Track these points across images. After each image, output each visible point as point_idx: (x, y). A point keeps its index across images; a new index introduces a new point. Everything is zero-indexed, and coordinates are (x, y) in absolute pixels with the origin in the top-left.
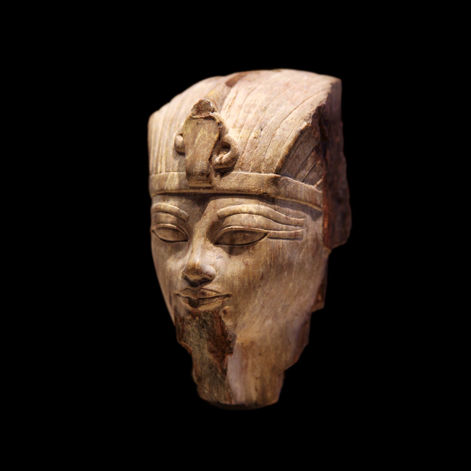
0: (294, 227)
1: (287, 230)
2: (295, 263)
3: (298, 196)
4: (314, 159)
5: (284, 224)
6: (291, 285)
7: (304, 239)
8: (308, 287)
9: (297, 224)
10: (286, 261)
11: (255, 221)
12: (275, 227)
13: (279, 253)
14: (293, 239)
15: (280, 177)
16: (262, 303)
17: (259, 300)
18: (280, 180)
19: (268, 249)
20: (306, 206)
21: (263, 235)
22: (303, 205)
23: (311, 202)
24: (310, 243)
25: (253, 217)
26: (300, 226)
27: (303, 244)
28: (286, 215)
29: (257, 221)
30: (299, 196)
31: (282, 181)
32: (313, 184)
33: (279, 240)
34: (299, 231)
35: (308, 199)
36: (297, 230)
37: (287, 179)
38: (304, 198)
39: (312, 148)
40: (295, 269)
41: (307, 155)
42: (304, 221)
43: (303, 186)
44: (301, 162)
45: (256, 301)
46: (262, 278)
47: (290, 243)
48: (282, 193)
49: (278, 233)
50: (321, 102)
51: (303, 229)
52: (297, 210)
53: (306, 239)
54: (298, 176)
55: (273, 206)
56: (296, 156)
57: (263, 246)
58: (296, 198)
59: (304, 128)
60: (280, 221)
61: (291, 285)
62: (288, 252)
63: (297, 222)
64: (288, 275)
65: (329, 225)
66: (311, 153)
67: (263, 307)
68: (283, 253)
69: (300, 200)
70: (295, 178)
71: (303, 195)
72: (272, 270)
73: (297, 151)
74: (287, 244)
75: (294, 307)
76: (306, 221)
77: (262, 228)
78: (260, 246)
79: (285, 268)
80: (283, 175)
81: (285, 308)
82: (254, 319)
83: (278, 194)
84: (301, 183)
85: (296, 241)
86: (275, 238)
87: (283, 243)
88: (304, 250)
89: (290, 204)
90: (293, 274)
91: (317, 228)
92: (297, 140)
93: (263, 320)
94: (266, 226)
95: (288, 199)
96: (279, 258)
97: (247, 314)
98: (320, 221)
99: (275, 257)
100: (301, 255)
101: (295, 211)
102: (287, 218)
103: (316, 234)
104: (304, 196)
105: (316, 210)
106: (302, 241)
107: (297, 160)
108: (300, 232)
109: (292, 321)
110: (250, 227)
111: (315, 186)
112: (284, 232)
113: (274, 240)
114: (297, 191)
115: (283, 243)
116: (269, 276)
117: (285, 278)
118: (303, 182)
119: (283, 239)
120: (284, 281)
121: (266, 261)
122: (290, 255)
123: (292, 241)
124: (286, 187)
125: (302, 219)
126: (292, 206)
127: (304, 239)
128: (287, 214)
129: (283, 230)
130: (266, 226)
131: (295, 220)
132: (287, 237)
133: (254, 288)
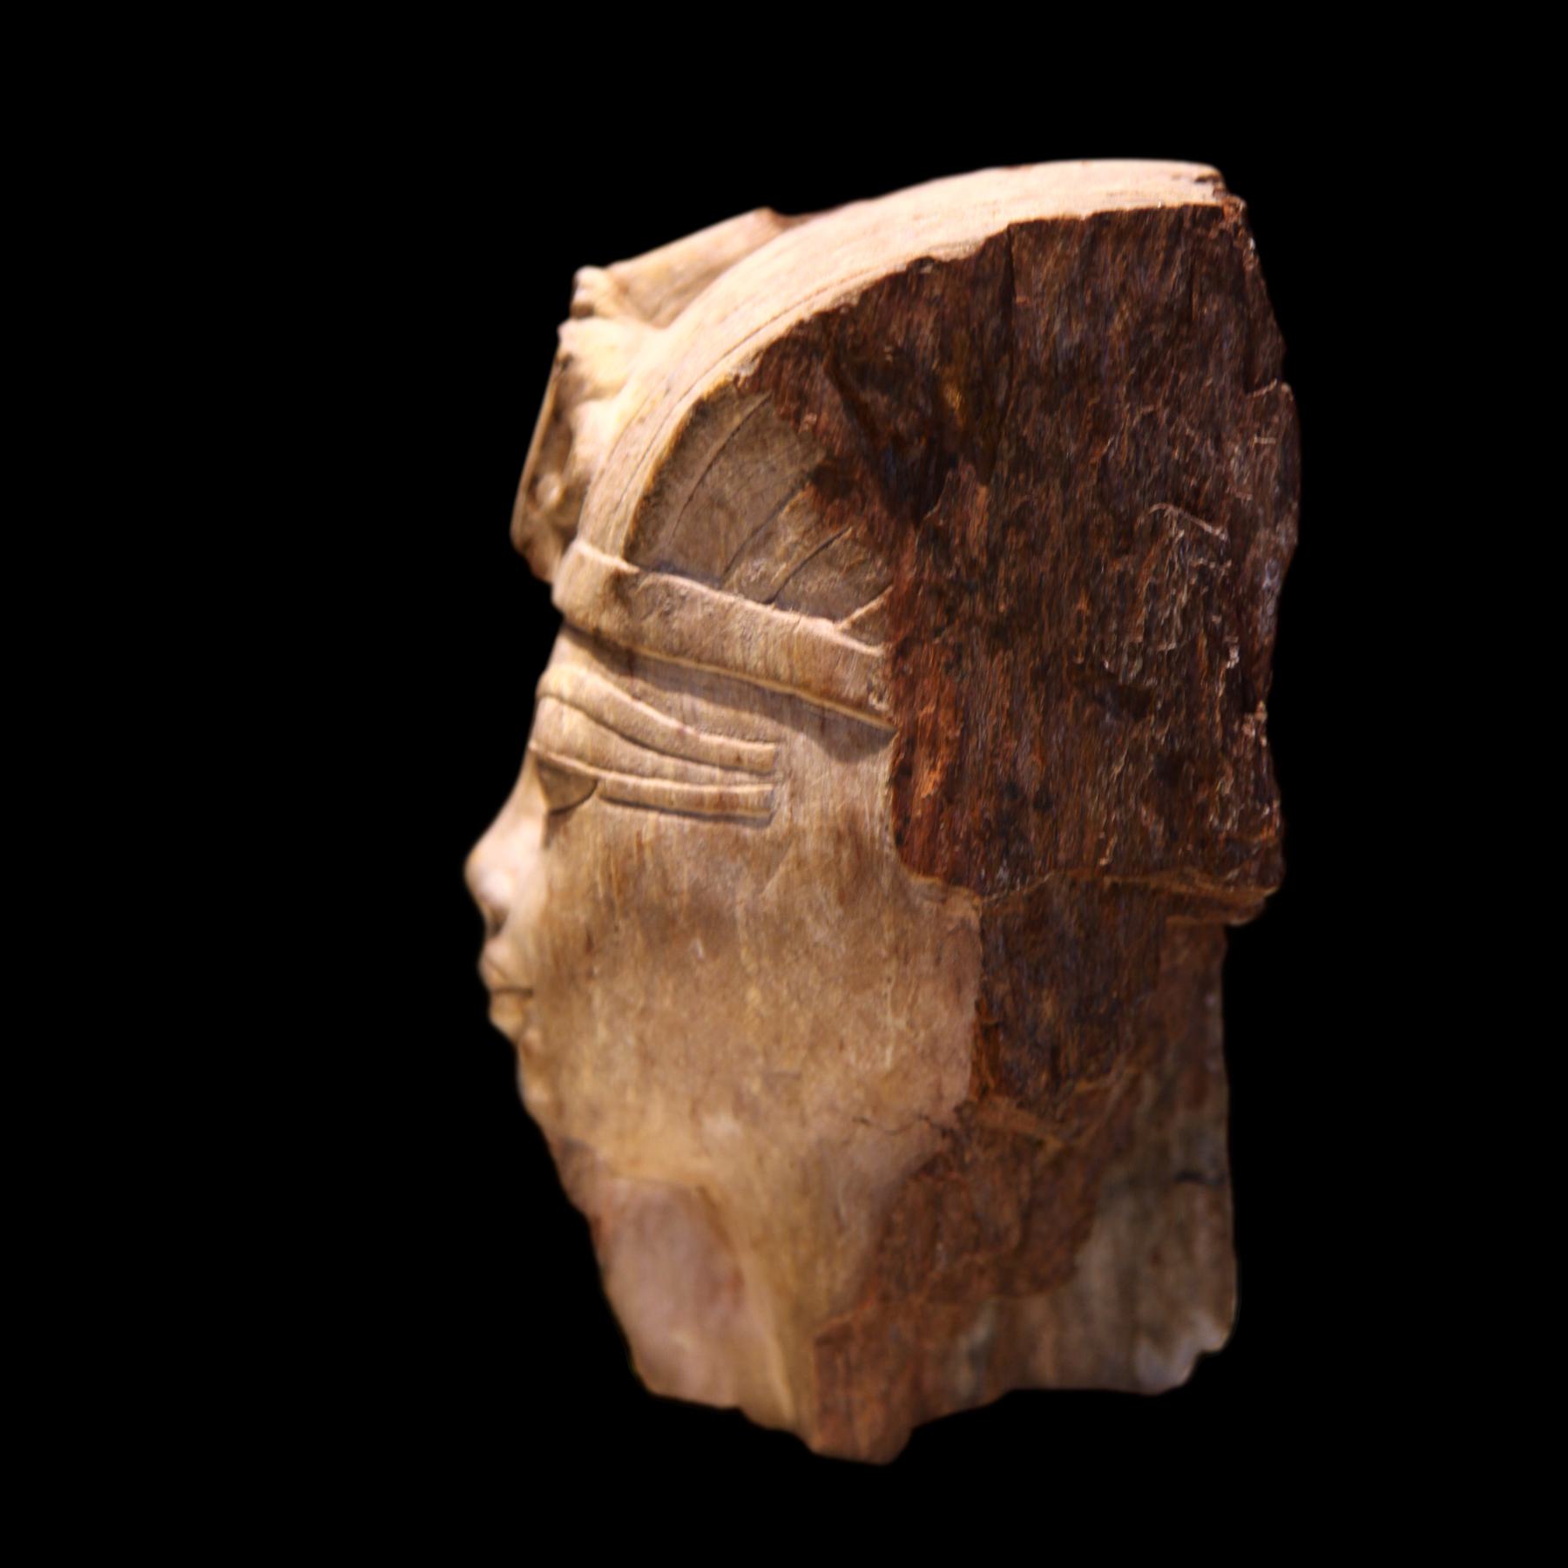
0: (717, 772)
1: (680, 777)
2: (739, 912)
3: (728, 654)
4: (813, 517)
5: (673, 755)
6: (753, 995)
7: (780, 824)
8: (870, 1021)
9: (734, 764)
10: (686, 898)
11: (559, 731)
12: (625, 762)
13: (642, 865)
14: (715, 819)
15: (637, 576)
16: (631, 1040)
17: (609, 1023)
18: (635, 585)
19: (599, 839)
20: (791, 697)
21: (590, 785)
22: (773, 694)
23: (806, 686)
24: (811, 844)
25: (561, 714)
26: (752, 772)
27: (779, 845)
28: (684, 720)
29: (566, 730)
30: (736, 653)
31: (647, 589)
32: (833, 618)
33: (640, 814)
34: (738, 790)
35: (783, 671)
36: (736, 784)
37: (667, 586)
38: (760, 664)
39: (791, 472)
40: (743, 935)
41: (772, 502)
42: (776, 756)
43: (762, 620)
44: (746, 527)
45: (602, 1033)
46: (589, 946)
47: (694, 830)
48: (652, 636)
49: (636, 789)
50: (847, 294)
51: (768, 788)
52: (737, 705)
53: (786, 825)
54: (734, 578)
55: (626, 681)
56: (711, 499)
57: (587, 828)
58: (723, 663)
59: (710, 396)
60: (648, 741)
61: (753, 995)
62: (687, 867)
63: (733, 756)
64: (714, 953)
65: (950, 789)
66: (793, 492)
67: (647, 1059)
68: (660, 864)
69: (743, 668)
70: (720, 583)
71: (755, 654)
72: (622, 924)
73: (708, 479)
74: (681, 832)
75: (828, 1085)
76: (791, 754)
77: (580, 757)
78: (581, 824)
79: (682, 921)
80: (648, 568)
81: (785, 1087)
82: (631, 1097)
83: (637, 636)
84: (760, 608)
85: (733, 828)
86: (626, 803)
87: (658, 827)
88: (782, 869)
89: (705, 682)
90: (743, 953)
91: (855, 790)
92: (684, 440)
93: (685, 1107)
94: (589, 754)
95: (685, 662)
96: (645, 881)
97: (586, 1073)
98: (880, 767)
99: (625, 877)
100: (771, 887)
101: (727, 713)
102: (680, 734)
103: (852, 818)
104: (764, 656)
105: (849, 720)
106: (768, 831)
107: (721, 517)
108: (746, 797)
109: (847, 1143)
110: (548, 748)
111: (845, 624)
112: (667, 785)
113: (617, 811)
114: (725, 636)
115: (658, 827)
116: (617, 944)
117: (700, 962)
118: (768, 602)
119: (663, 811)
120: (699, 971)
121: (594, 887)
122: (699, 874)
123: (706, 827)
124: (667, 613)
125: (770, 747)
126: (712, 691)
127: (780, 824)
128: (691, 718)
129: (664, 777)
130: (589, 754)
131: (721, 747)
132: (676, 806)
133: (573, 977)
